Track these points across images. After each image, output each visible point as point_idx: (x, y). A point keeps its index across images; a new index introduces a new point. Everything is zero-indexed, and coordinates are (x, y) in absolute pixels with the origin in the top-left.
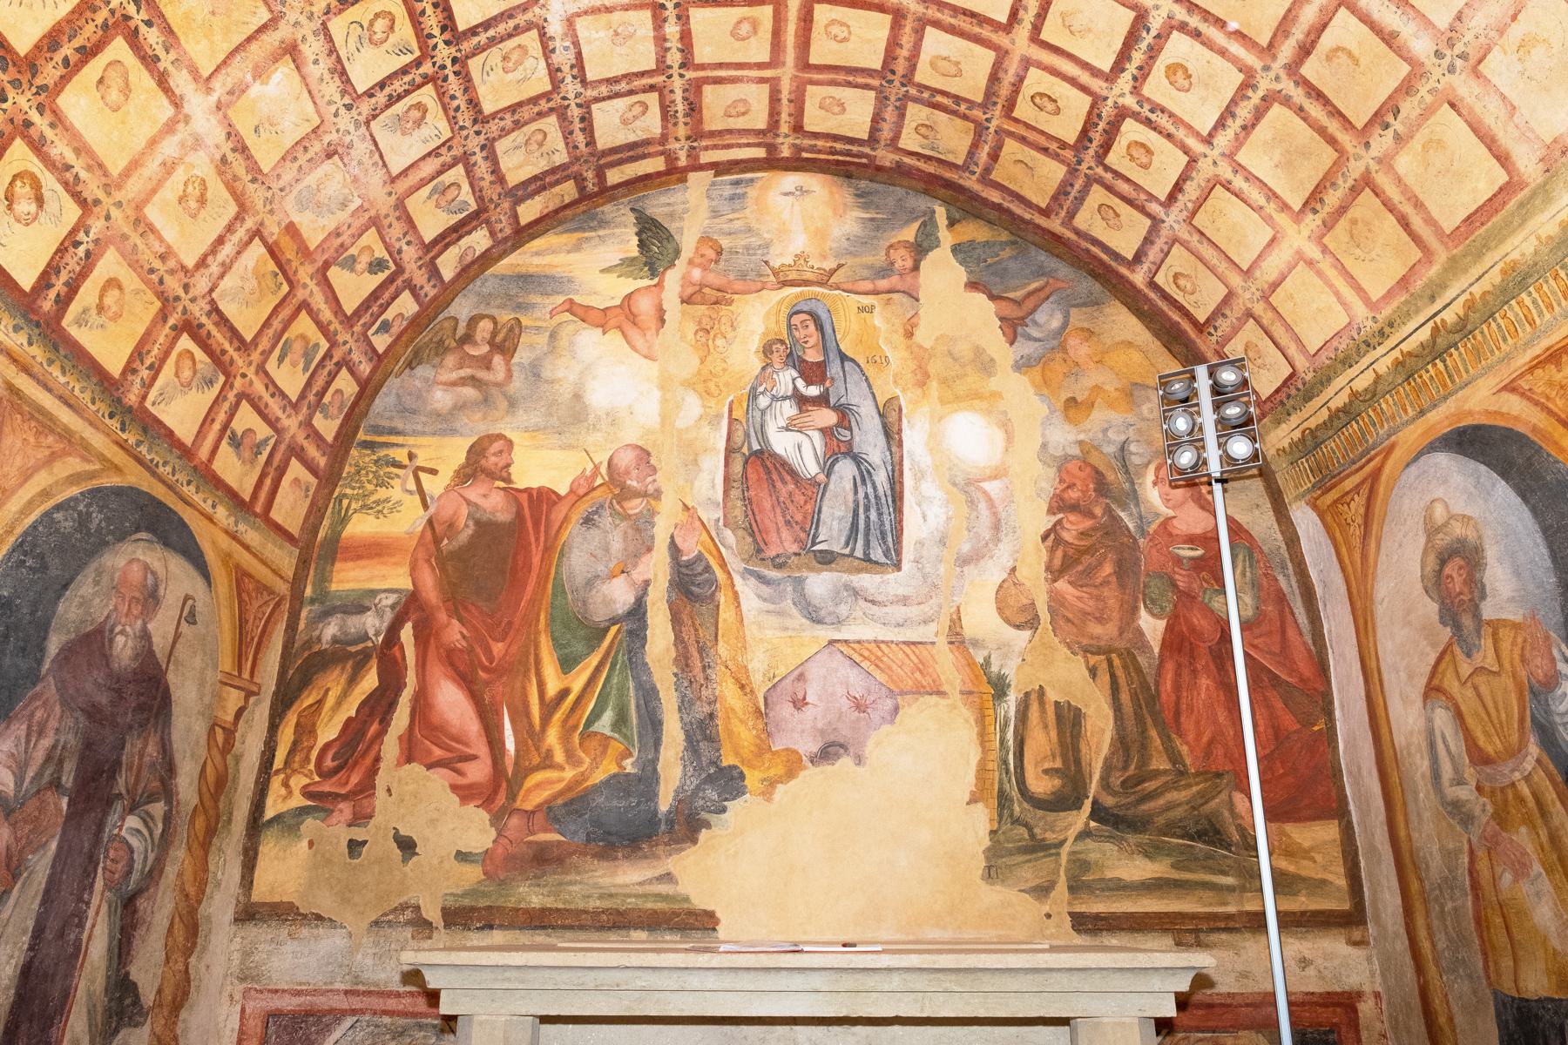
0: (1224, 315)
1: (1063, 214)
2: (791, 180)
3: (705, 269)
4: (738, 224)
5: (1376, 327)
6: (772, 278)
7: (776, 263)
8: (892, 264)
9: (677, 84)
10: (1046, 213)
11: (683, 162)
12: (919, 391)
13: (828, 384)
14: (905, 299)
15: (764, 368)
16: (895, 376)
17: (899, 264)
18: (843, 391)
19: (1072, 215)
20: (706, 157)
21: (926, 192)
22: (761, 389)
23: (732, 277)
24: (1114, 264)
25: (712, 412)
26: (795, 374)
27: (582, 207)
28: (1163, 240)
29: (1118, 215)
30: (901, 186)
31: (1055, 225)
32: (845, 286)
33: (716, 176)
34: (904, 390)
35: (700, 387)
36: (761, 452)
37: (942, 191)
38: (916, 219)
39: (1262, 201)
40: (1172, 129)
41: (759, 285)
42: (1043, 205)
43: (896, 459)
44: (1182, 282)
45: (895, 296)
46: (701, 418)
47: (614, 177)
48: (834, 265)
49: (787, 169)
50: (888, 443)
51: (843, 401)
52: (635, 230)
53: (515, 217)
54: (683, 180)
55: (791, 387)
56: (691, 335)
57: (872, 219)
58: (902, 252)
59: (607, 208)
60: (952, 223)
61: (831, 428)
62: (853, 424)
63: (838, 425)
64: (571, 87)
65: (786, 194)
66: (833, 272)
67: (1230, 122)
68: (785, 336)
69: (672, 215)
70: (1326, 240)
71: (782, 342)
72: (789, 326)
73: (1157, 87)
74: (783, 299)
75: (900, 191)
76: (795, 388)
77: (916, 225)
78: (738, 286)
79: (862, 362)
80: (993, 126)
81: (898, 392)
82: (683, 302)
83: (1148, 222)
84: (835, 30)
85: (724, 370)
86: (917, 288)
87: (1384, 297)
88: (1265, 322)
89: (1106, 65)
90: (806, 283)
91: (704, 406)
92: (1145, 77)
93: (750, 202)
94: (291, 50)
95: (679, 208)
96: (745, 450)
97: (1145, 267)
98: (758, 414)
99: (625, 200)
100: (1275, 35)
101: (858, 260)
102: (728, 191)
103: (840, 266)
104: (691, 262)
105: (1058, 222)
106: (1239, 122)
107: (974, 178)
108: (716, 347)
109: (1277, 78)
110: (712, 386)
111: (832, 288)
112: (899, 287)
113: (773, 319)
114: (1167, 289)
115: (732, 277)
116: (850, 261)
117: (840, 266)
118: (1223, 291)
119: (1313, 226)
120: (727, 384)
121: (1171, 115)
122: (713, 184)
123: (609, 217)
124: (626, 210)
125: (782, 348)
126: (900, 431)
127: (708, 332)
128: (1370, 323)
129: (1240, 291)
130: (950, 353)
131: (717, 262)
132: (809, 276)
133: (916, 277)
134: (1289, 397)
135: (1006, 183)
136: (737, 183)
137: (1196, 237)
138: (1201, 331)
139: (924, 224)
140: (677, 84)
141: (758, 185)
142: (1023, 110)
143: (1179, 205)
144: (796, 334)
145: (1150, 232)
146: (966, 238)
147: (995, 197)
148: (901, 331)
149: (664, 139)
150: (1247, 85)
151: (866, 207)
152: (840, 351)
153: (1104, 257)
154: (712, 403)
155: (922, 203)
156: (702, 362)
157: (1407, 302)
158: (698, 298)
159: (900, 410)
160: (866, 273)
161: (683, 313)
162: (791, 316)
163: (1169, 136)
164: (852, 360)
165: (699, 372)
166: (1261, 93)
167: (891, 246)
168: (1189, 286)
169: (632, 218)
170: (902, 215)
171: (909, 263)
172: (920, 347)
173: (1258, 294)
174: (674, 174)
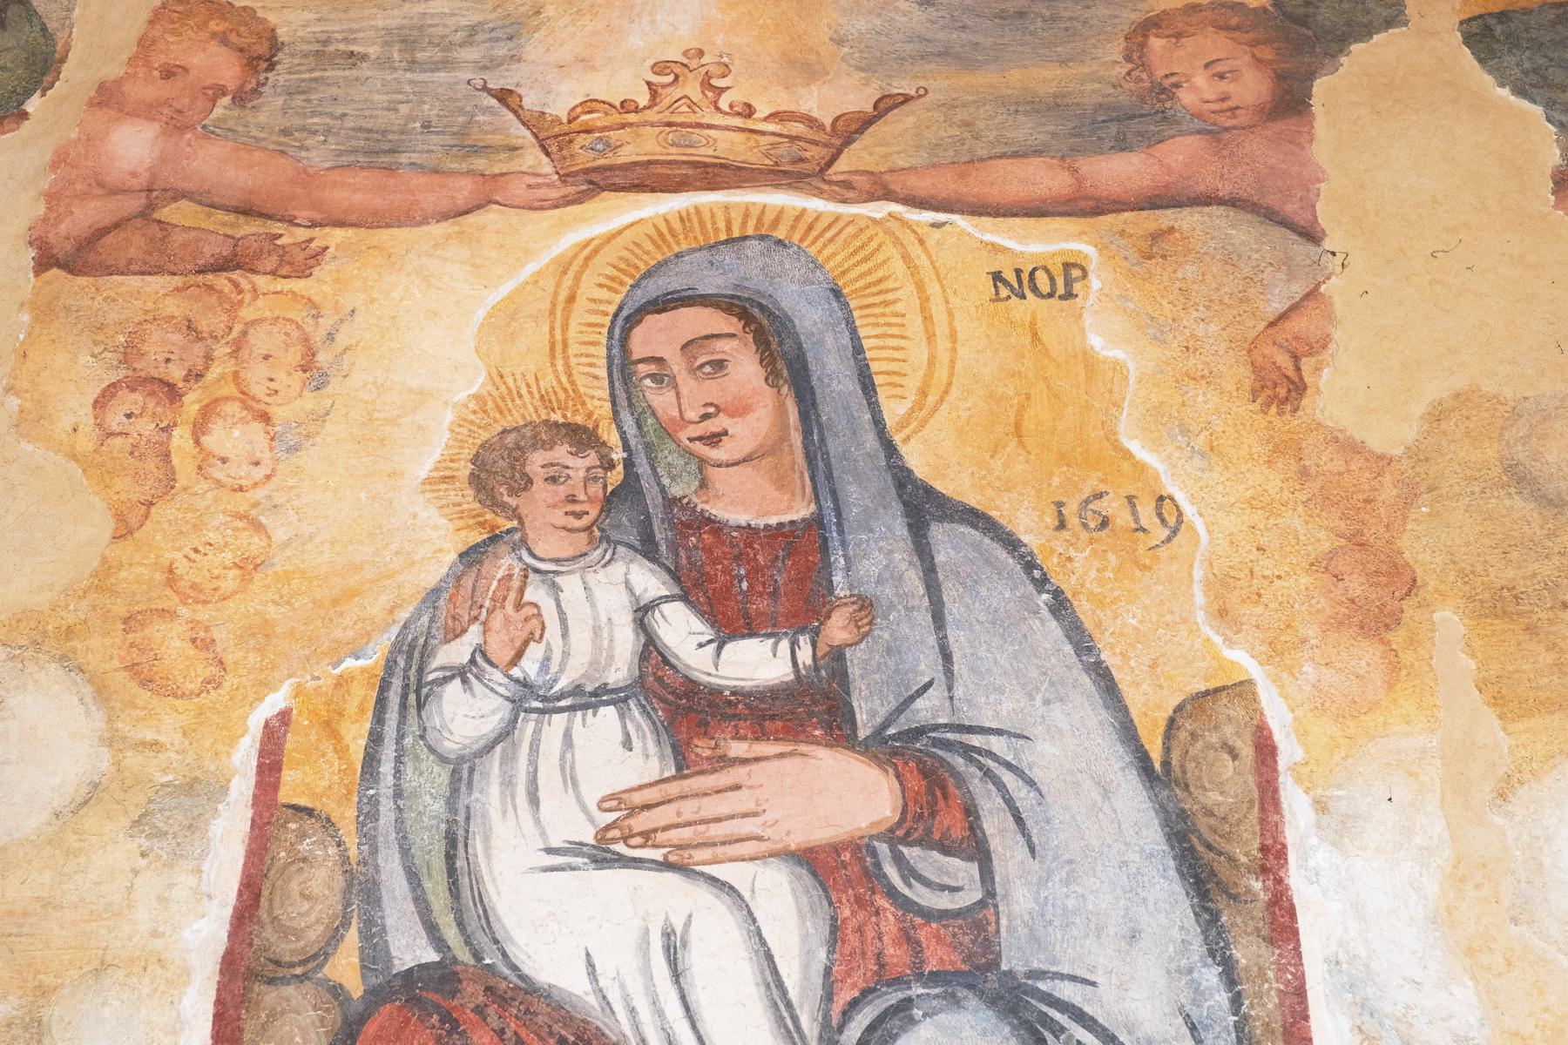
3: (177, 125)
6: (533, 158)
7: (560, 101)
8: (1165, 91)
12: (1367, 655)
13: (837, 629)
14: (1241, 232)
15: (471, 557)
16: (1220, 585)
17: (1198, 91)
18: (926, 665)
22: (457, 652)
23: (318, 157)
25: (161, 771)
26: (649, 581)
32: (921, 185)
34: (1275, 652)
35: (103, 650)
36: (444, 976)
41: (464, 190)
43: (1266, 1006)
45: (1187, 220)
46: (91, 796)
48: (859, 100)
50: (1209, 920)
51: (928, 708)
55: (626, 641)
56: (75, 408)
58: (1212, 44)
61: (860, 848)
62: (994, 822)
63: (897, 835)
66: (852, 128)
68: (597, 404)
71: (581, 437)
72: (622, 367)
74: (590, 251)
76: (651, 650)
78: (353, 191)
79: (1030, 527)
81: (1243, 661)
82: (46, 261)
85: (248, 567)
86: (1307, 185)
90: (714, 175)
91: (112, 740)
96: (346, 968)
98: (428, 783)
101: (985, 79)
103: (886, 105)
104: (107, 97)
108: (205, 460)
110: (171, 642)
111: (846, 190)
112: (1209, 178)
113: (535, 337)
115: (318, 157)
116: (941, 83)
117: (886, 105)
120: (261, 632)
125: (581, 465)
126: (1273, 857)
127: (172, 392)
130: (1518, 477)
131: (241, 98)
132: (727, 145)
133: (1301, 139)
144: (661, 401)
148: (1236, 373)
152: (903, 479)
154: (168, 723)
156: (123, 530)
158: (135, 244)
159: (1265, 750)
160: (1025, 130)
161: (44, 311)
162: (627, 322)
164: (974, 517)
165: (102, 579)
167: (1152, 25)
171: (1252, 87)
172: (1351, 448)
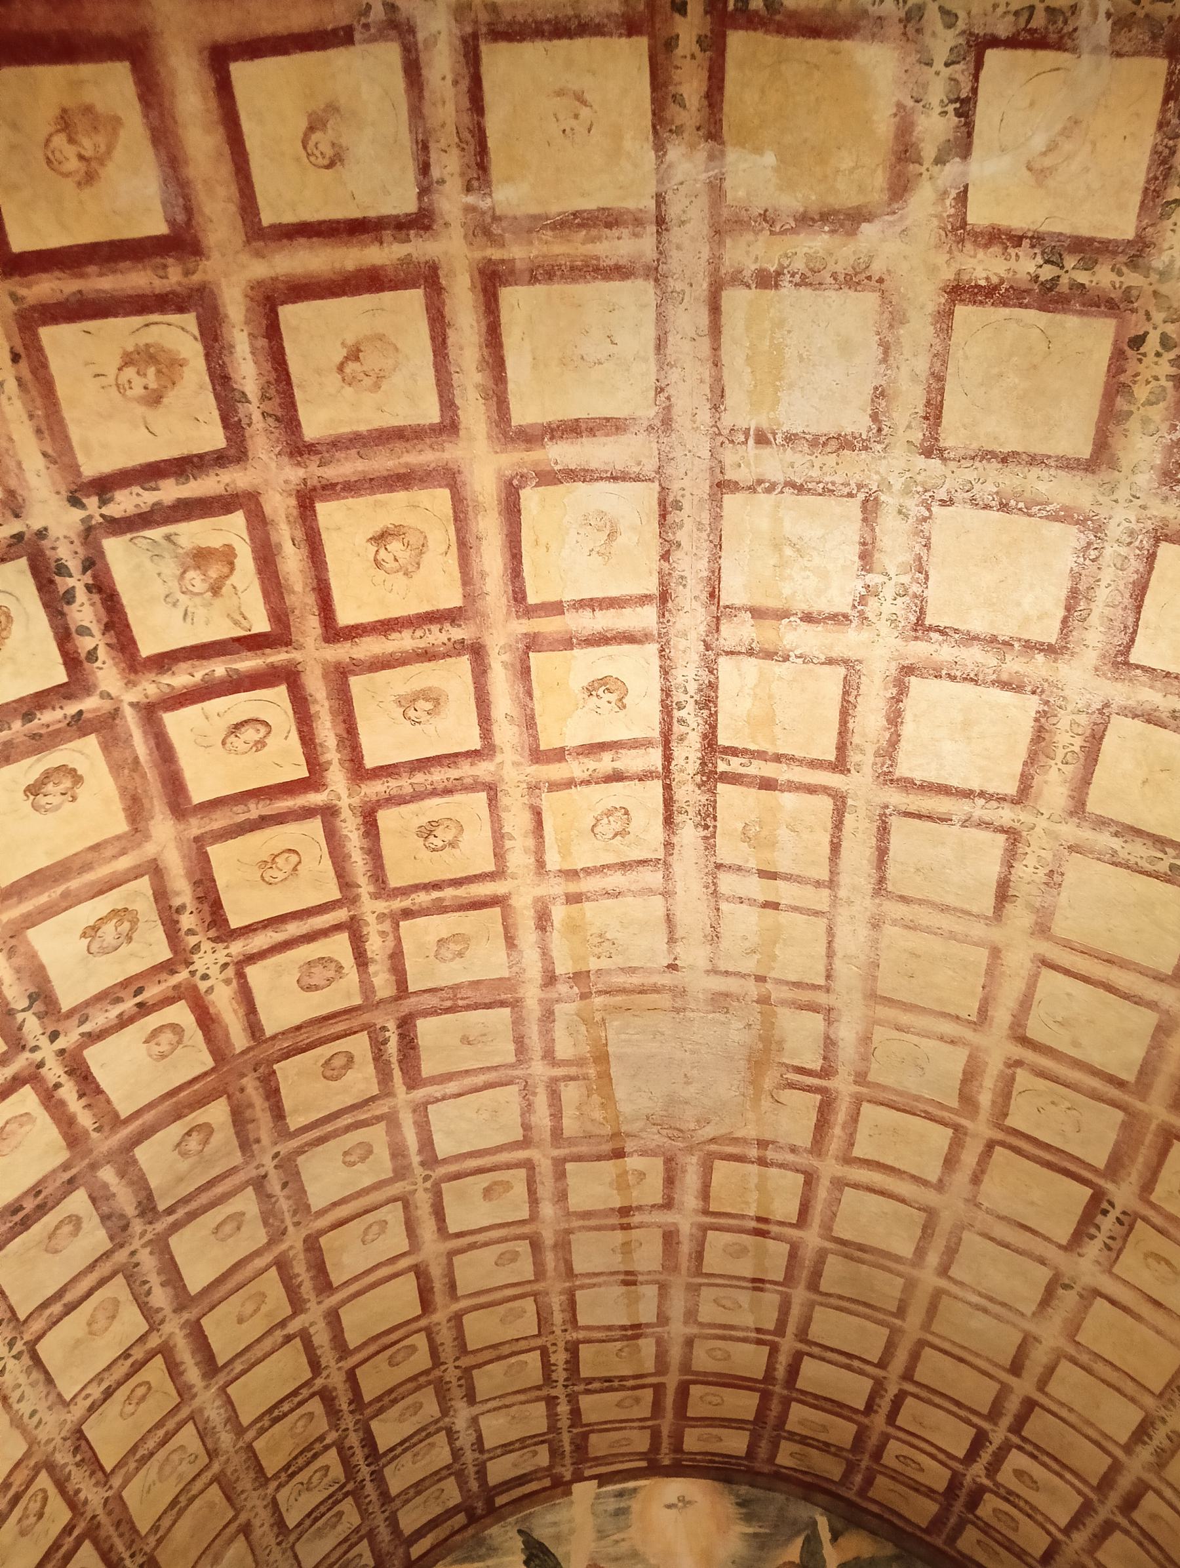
2: (675, 1488)
4: (624, 1547)
9: (566, 1438)
10: (926, 1531)
11: (568, 1476)
19: (952, 1539)
20: (587, 1473)
21: (806, 1499)
27: (471, 1531)
30: (781, 1492)
31: (939, 1542)
33: (600, 1486)
37: (820, 1498)
38: (798, 1533)
47: (500, 1501)
49: (668, 1475)
52: (523, 1557)
53: (408, 1555)
54: (569, 1493)
57: (756, 1535)
59: (494, 1530)
60: (835, 1538)
64: (469, 1456)
65: (669, 1507)
69: (558, 1537)
73: (1005, 1476)
75: (780, 1497)
77: (799, 1542)
80: (864, 1464)
84: (709, 1398)
89: (961, 1454)
93: (633, 1517)
94: (246, 1530)
95: (565, 1528)
99: (511, 1520)
102: (612, 1505)
122: (598, 1496)
123: (496, 1543)
124: (513, 1533)
136: (620, 1494)
139: (807, 1540)
140: (566, 1438)
141: (641, 1495)
142: (888, 1459)
146: (849, 1556)
147: (875, 1508)
149: (551, 1467)
150: (1087, 1508)
151: (748, 1518)
155: (802, 1511)
169: (518, 1543)
170: (784, 1529)
174: (560, 1487)
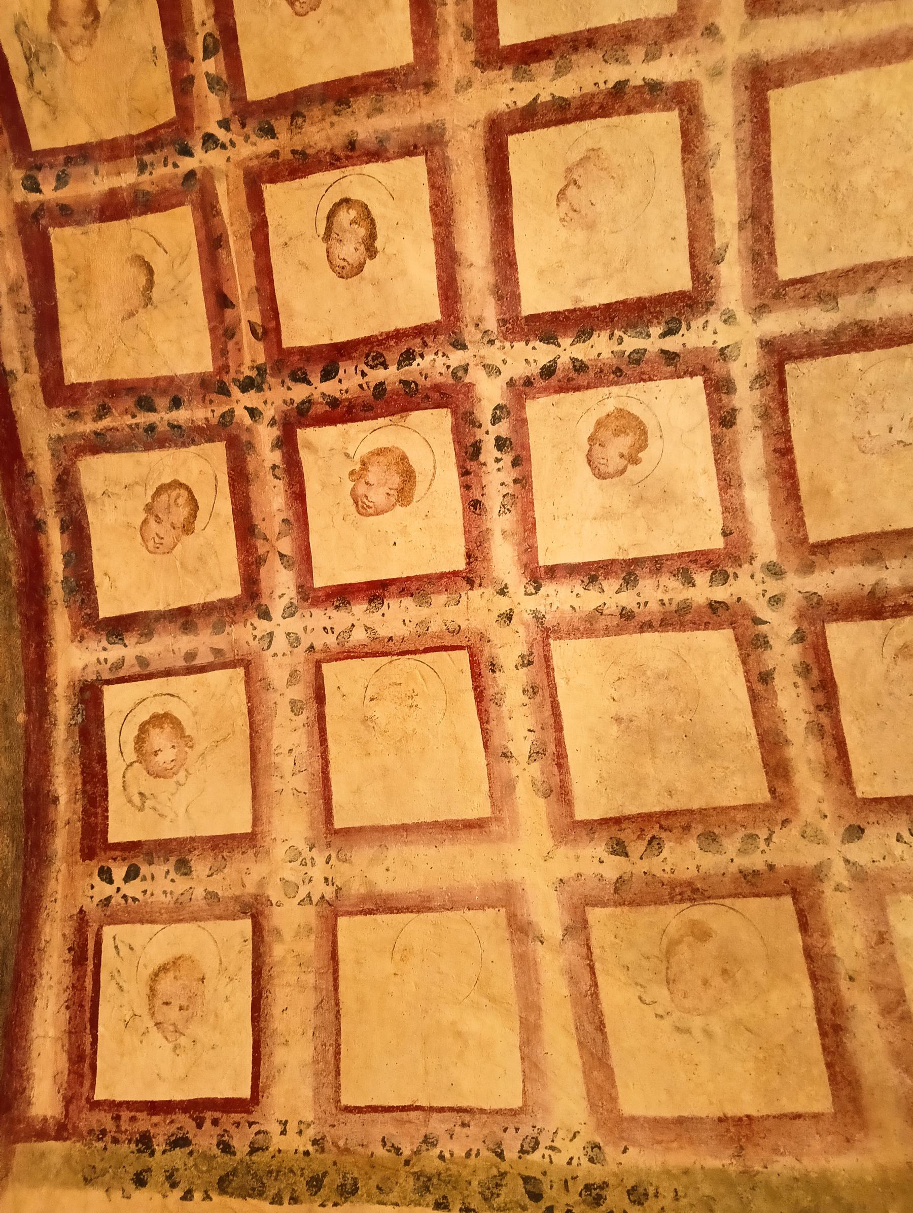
0: (183, 867)
1: (88, 426)
5: (588, 1172)
24: (57, 592)
28: (220, 641)
29: (188, 528)
39: (521, 746)
40: (493, 500)
42: (72, 376)
44: (159, 738)
67: (611, 585)
70: (595, 915)
83: (232, 589)
87: (657, 1124)
88: (277, 951)
92: (568, 386)
97: (115, 652)
100: (851, 541)
105: (58, 430)
106: (628, 599)
107: (20, 195)
109: (776, 601)
114: (111, 727)
118: (243, 826)
119: (590, 869)
121: (524, 482)
128: (576, 1149)
129: (279, 852)
134: (179, 1142)
135: (61, 270)
137: (300, 692)
138: (88, 853)
143: (340, 618)
145: (208, 609)
153: (57, 566)
157: (720, 1177)
163: (474, 506)
166: (720, 593)
168: (167, 756)
173: (319, 889)
